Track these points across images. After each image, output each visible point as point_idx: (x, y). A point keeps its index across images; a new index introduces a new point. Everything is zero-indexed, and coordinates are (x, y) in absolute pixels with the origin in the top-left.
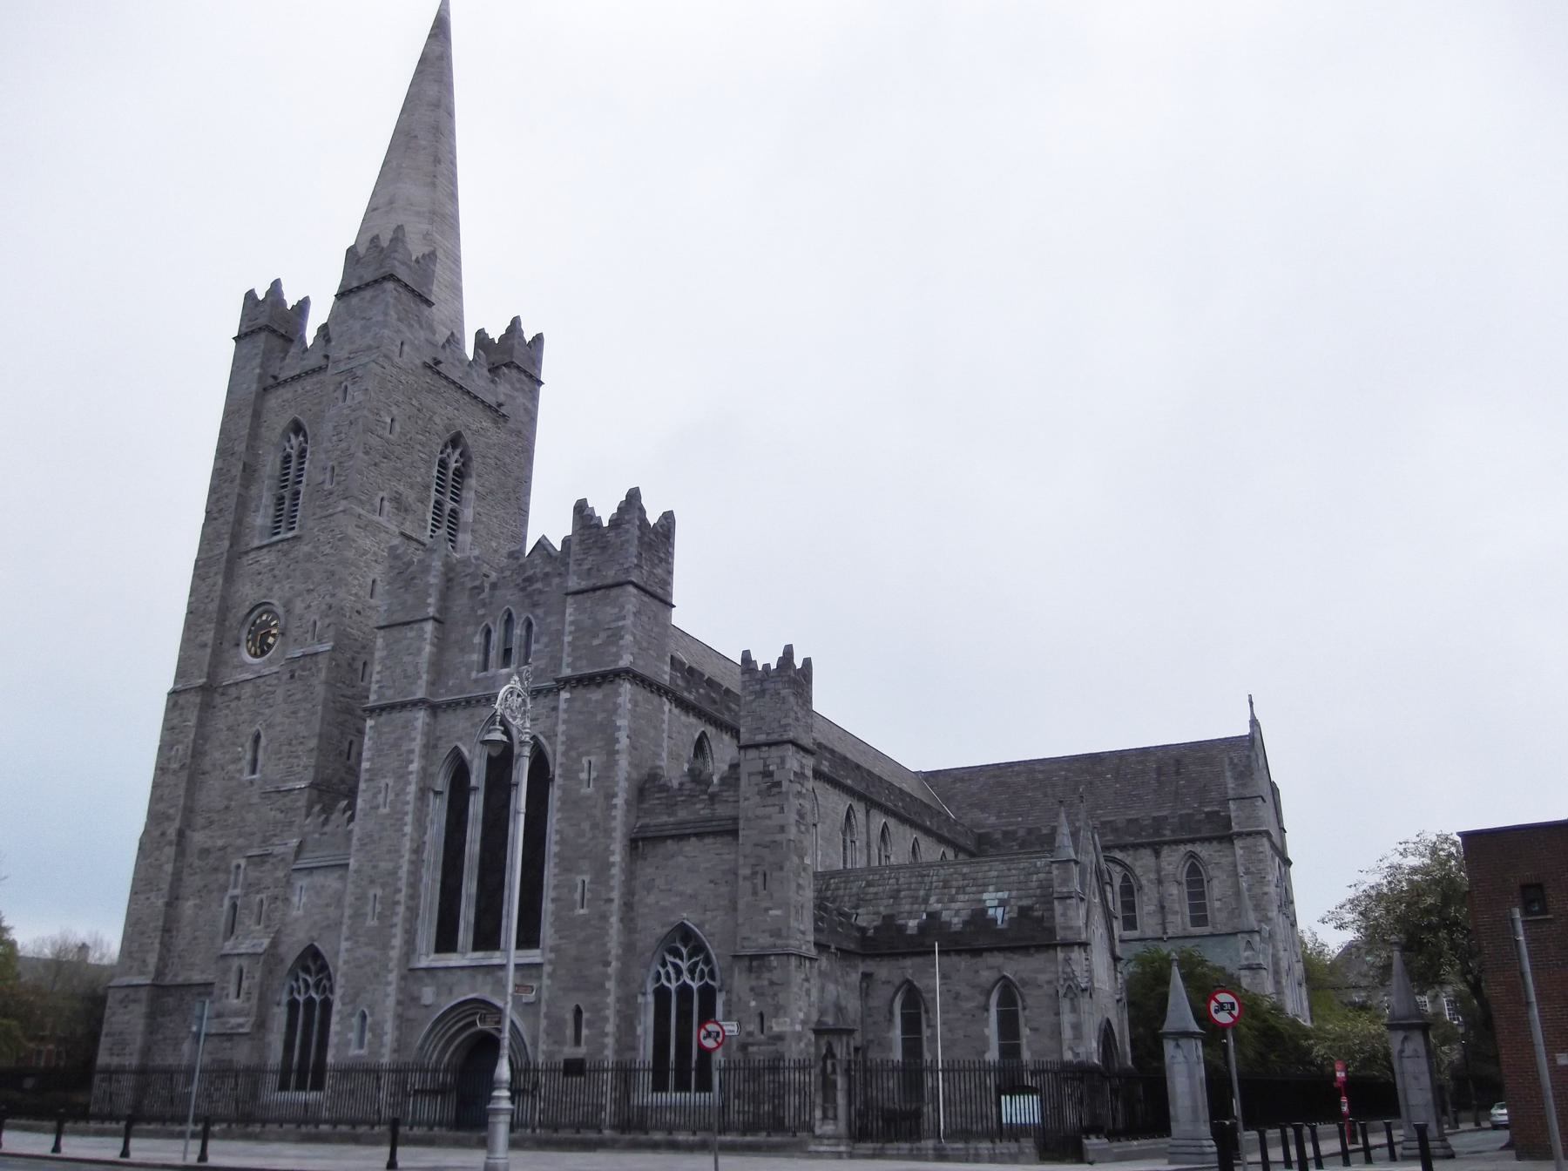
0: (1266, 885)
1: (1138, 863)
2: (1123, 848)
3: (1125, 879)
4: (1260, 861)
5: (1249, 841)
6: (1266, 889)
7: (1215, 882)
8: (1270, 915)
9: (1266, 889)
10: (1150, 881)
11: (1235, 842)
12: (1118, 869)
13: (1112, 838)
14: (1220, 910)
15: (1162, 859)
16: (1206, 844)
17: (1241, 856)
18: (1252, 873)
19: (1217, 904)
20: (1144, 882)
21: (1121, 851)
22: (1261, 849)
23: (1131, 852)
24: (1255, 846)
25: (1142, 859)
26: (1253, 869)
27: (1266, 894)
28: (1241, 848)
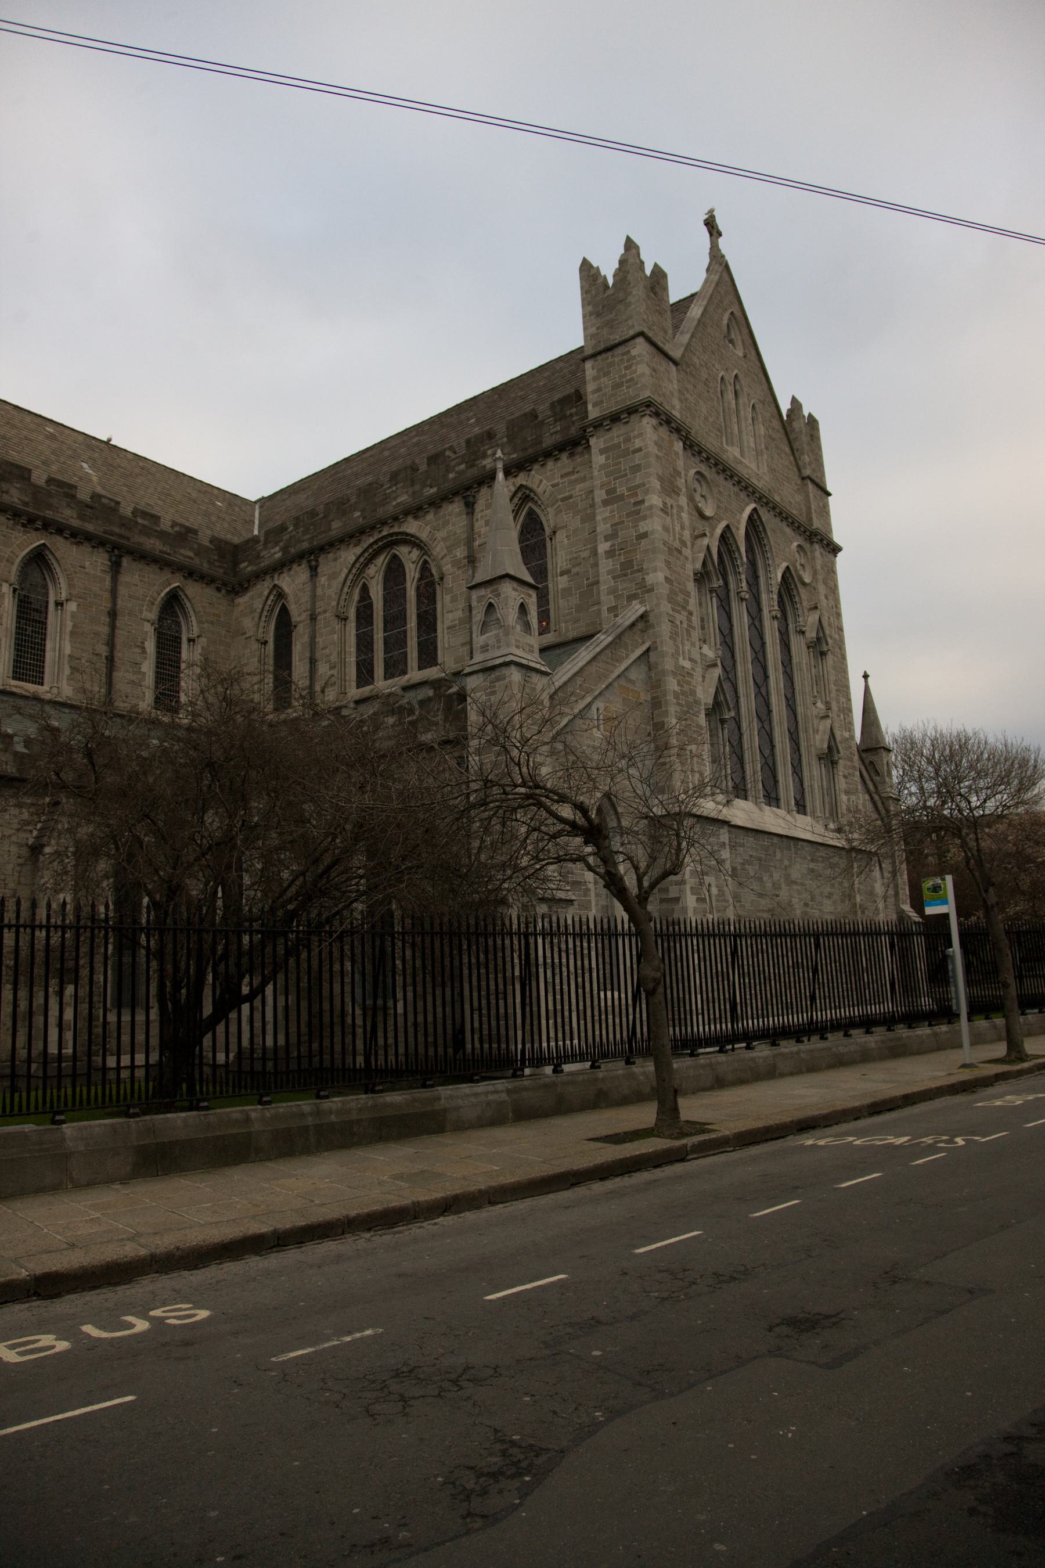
0: (644, 518)
1: (440, 535)
2: (415, 511)
3: (425, 568)
4: (636, 468)
5: (617, 433)
6: (644, 526)
7: (560, 536)
8: (650, 579)
9: (644, 526)
10: (456, 563)
11: (593, 441)
12: (415, 553)
13: (403, 498)
14: (567, 592)
15: (478, 515)
16: (550, 464)
17: (602, 467)
18: (621, 498)
19: (563, 582)
20: (448, 568)
21: (416, 518)
22: (638, 443)
23: (430, 516)
24: (627, 440)
25: (446, 523)
26: (622, 490)
27: (644, 535)
28: (602, 452)
